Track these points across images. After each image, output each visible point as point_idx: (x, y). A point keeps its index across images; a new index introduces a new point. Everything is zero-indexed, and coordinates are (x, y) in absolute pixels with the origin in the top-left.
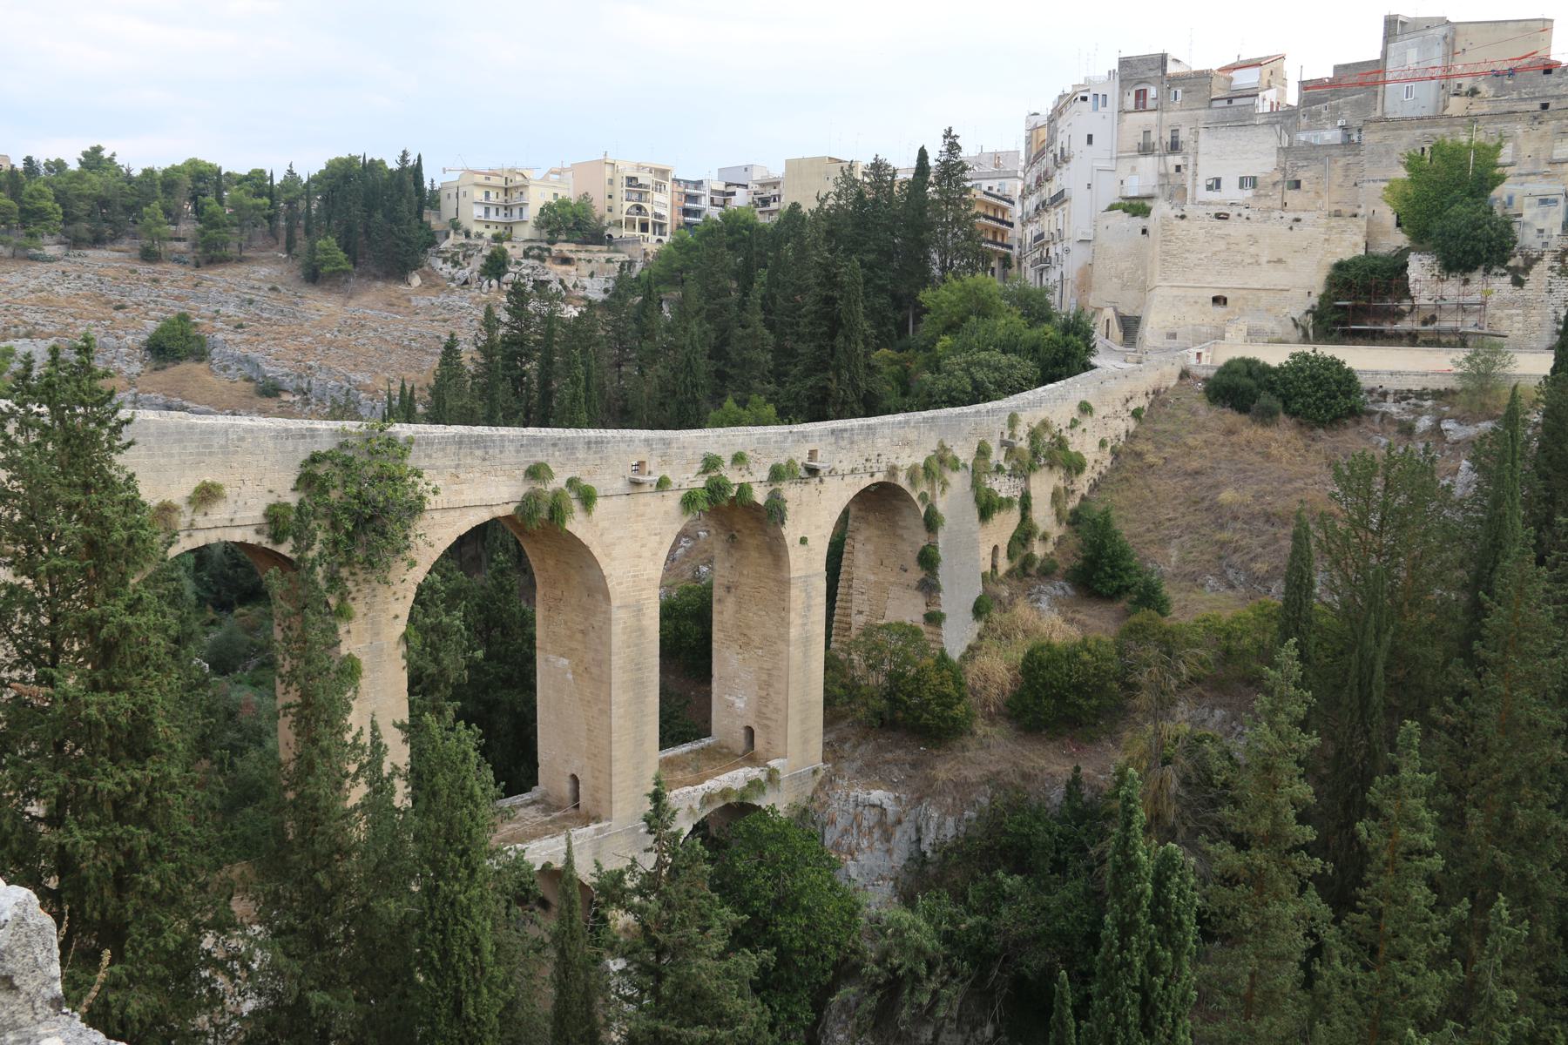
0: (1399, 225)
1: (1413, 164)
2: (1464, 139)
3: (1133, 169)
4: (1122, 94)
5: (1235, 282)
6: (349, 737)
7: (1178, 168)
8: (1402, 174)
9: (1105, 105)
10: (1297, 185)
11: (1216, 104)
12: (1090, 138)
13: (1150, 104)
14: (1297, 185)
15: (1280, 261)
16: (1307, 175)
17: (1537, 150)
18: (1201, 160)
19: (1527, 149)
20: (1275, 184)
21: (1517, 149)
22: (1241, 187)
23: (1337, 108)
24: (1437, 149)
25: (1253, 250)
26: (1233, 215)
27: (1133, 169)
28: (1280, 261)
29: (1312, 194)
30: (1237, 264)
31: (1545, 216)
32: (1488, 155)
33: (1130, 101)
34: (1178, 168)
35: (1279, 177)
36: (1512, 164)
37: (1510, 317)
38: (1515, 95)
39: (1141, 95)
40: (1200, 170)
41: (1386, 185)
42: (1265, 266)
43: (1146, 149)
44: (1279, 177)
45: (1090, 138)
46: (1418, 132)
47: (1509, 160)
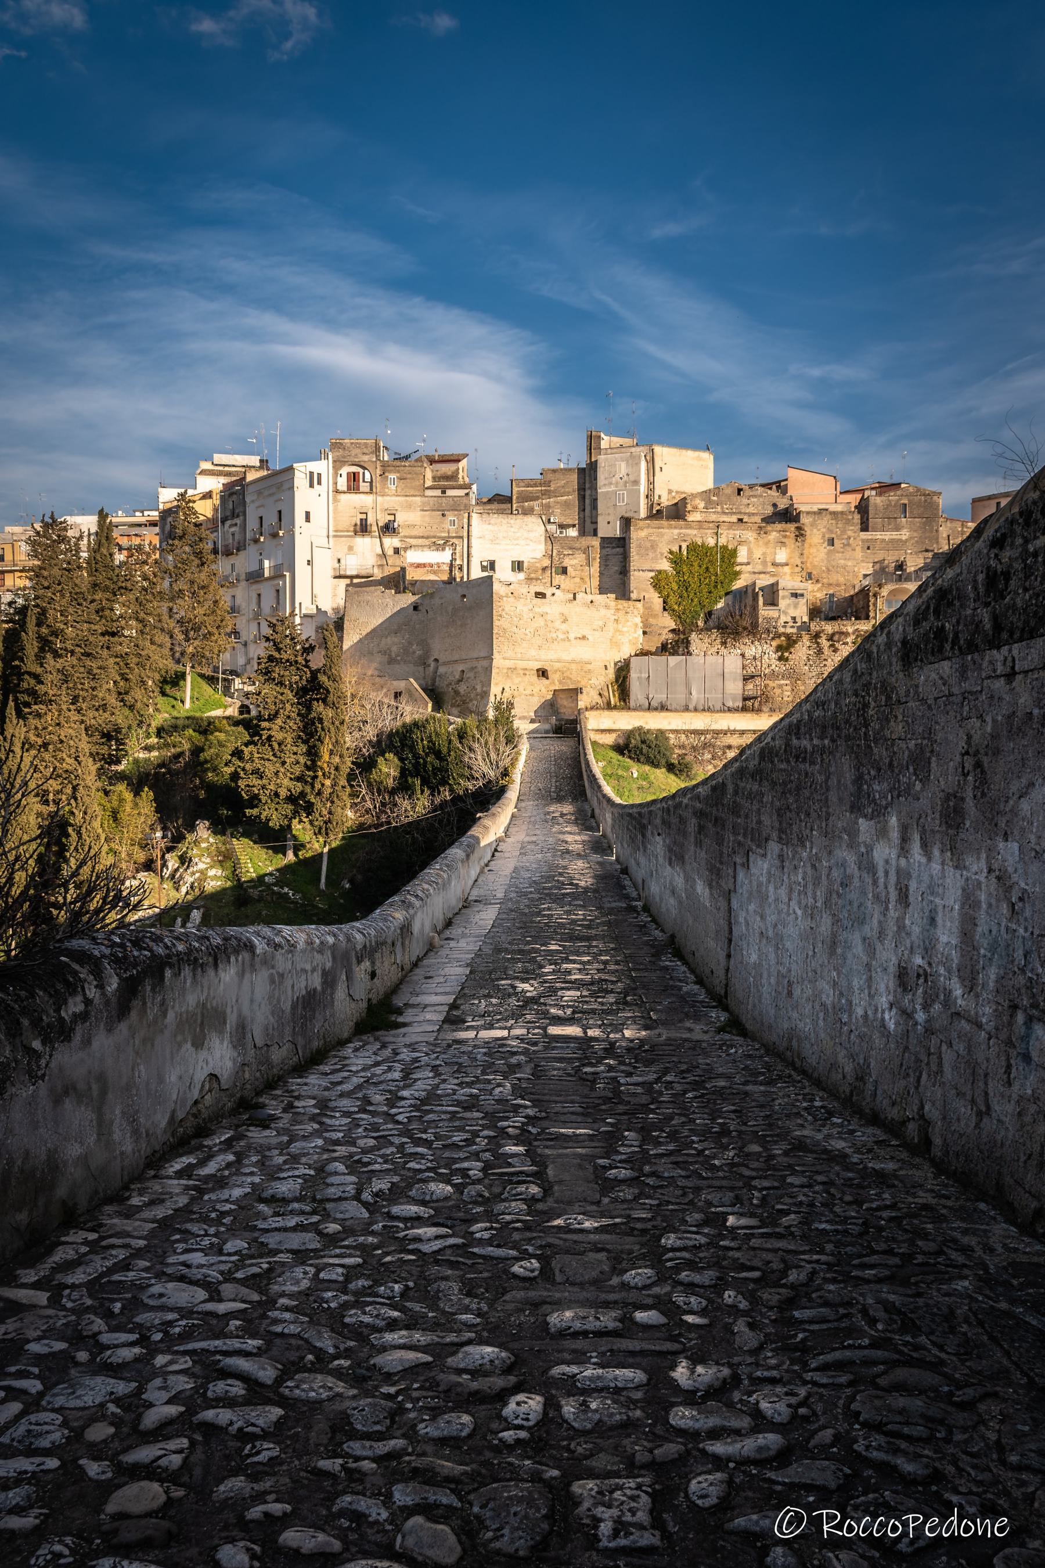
0: (665, 609)
1: (676, 560)
2: (711, 542)
3: (351, 548)
4: (336, 474)
5: (551, 655)
6: (396, 1179)
7: (397, 551)
8: (665, 566)
9: (319, 483)
10: (564, 571)
11: (429, 493)
12: (308, 514)
13: (364, 487)
14: (564, 571)
15: (584, 638)
16: (574, 562)
17: (764, 554)
18: (474, 542)
19: (758, 553)
20: (544, 569)
21: (750, 552)
22: (513, 570)
23: (548, 506)
24: (693, 548)
25: (564, 627)
26: (548, 593)
27: (351, 548)
28: (584, 638)
29: (577, 580)
30: (553, 640)
31: (796, 606)
32: (729, 555)
33: (342, 483)
34: (397, 551)
35: (547, 562)
36: (748, 564)
37: (780, 686)
38: (719, 509)
39: (354, 478)
40: (473, 551)
41: (653, 574)
42: (574, 642)
43: (363, 528)
44: (547, 562)
45: (308, 514)
46: (676, 531)
47: (784, 561)
